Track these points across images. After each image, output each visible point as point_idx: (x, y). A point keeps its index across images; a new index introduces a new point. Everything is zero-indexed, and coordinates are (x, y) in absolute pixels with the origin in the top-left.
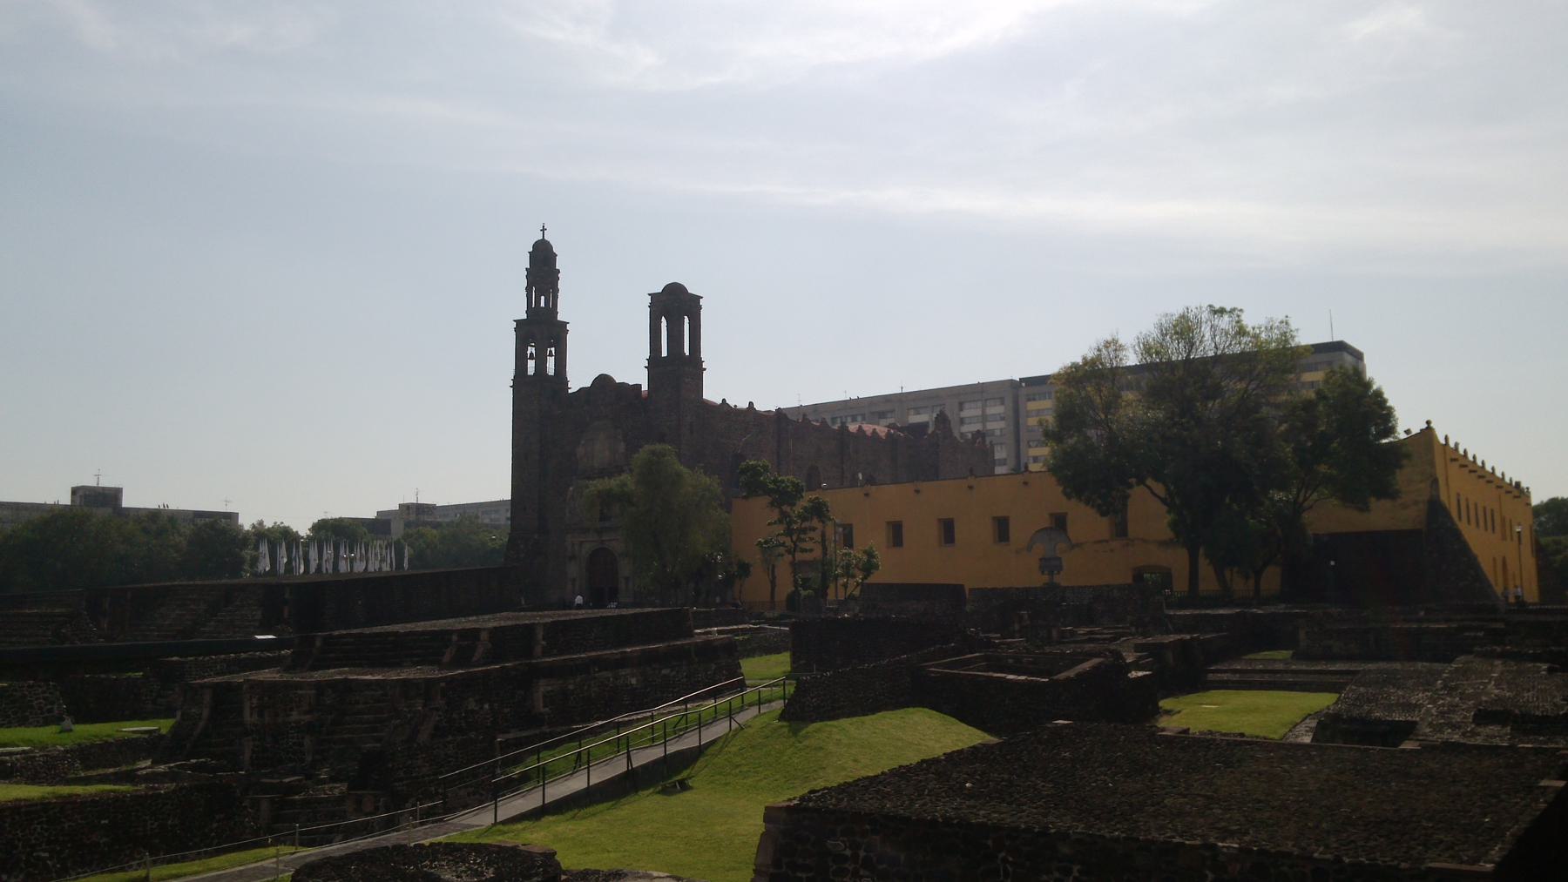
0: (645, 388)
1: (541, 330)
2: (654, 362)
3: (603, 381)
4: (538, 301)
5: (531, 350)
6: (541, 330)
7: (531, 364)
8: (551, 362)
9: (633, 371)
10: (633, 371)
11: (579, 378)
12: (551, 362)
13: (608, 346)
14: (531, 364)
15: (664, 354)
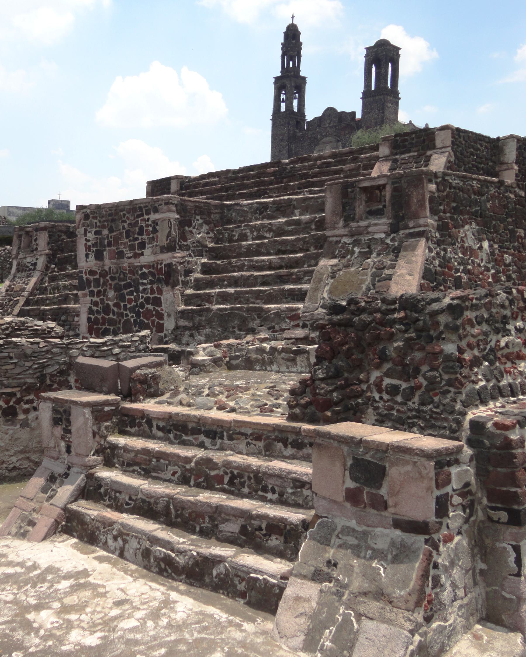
0: (359, 116)
1: (290, 82)
2: (367, 95)
3: (330, 112)
4: (288, 64)
5: (283, 96)
6: (290, 82)
7: (283, 105)
8: (295, 102)
9: (352, 103)
10: (352, 103)
11: (313, 111)
12: (295, 102)
13: (335, 88)
14: (283, 105)
15: (373, 88)
